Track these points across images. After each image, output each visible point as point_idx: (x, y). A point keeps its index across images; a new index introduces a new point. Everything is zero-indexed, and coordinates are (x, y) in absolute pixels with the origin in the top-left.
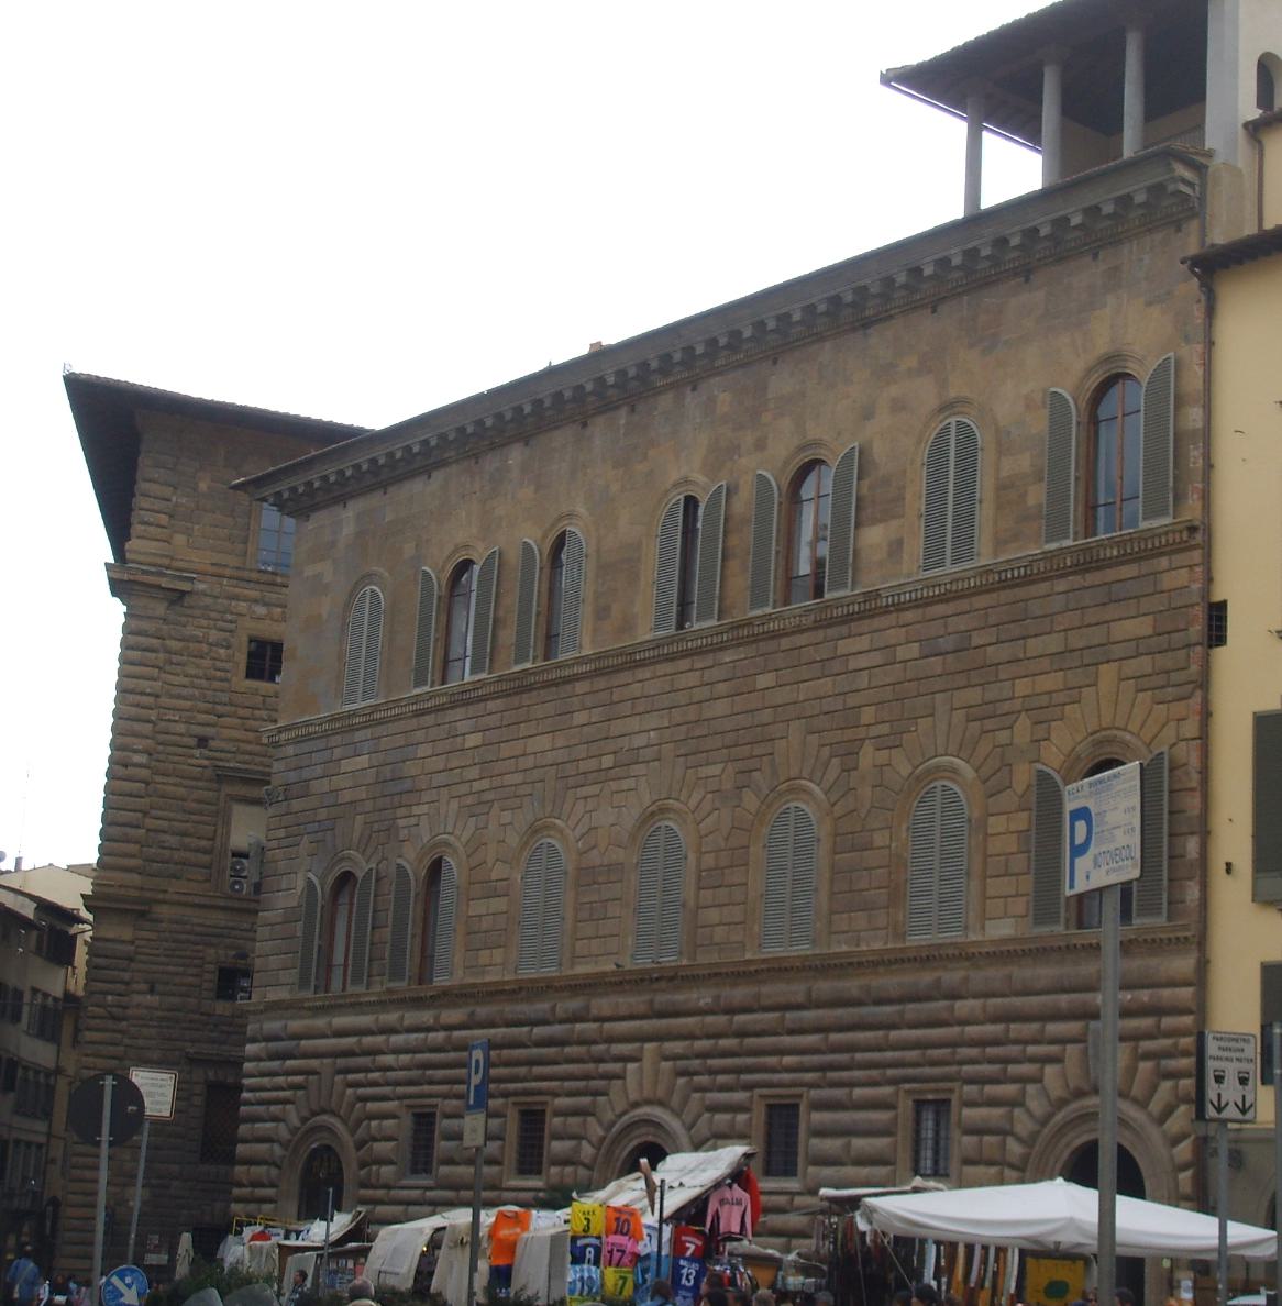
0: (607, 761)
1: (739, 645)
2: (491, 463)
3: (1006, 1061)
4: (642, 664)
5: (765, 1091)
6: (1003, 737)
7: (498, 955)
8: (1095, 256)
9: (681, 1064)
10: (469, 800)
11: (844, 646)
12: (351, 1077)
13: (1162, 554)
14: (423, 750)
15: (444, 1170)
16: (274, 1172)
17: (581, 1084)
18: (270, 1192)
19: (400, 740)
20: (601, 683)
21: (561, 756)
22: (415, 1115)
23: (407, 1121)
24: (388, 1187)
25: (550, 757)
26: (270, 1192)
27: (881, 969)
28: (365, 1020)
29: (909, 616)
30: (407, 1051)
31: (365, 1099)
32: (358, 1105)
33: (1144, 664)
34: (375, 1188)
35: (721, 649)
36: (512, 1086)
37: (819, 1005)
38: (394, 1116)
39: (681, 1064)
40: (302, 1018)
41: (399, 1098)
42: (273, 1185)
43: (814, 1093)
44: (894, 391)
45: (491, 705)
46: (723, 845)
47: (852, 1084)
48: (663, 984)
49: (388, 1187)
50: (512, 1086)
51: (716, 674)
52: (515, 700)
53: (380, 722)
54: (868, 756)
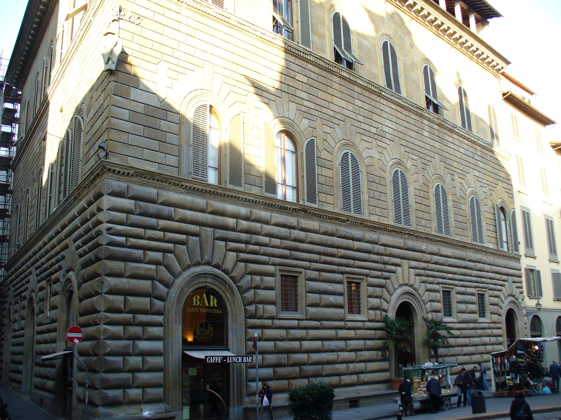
0: (373, 130)
7: (330, 199)
12: (232, 245)
15: (312, 310)
16: (159, 304)
17: (379, 273)
18: (159, 319)
24: (272, 318)
28: (243, 210)
30: (276, 237)
34: (260, 318)
36: (348, 269)
38: (272, 275)
40: (177, 192)
42: (159, 313)
45: (310, 66)
49: (272, 318)
50: (348, 269)
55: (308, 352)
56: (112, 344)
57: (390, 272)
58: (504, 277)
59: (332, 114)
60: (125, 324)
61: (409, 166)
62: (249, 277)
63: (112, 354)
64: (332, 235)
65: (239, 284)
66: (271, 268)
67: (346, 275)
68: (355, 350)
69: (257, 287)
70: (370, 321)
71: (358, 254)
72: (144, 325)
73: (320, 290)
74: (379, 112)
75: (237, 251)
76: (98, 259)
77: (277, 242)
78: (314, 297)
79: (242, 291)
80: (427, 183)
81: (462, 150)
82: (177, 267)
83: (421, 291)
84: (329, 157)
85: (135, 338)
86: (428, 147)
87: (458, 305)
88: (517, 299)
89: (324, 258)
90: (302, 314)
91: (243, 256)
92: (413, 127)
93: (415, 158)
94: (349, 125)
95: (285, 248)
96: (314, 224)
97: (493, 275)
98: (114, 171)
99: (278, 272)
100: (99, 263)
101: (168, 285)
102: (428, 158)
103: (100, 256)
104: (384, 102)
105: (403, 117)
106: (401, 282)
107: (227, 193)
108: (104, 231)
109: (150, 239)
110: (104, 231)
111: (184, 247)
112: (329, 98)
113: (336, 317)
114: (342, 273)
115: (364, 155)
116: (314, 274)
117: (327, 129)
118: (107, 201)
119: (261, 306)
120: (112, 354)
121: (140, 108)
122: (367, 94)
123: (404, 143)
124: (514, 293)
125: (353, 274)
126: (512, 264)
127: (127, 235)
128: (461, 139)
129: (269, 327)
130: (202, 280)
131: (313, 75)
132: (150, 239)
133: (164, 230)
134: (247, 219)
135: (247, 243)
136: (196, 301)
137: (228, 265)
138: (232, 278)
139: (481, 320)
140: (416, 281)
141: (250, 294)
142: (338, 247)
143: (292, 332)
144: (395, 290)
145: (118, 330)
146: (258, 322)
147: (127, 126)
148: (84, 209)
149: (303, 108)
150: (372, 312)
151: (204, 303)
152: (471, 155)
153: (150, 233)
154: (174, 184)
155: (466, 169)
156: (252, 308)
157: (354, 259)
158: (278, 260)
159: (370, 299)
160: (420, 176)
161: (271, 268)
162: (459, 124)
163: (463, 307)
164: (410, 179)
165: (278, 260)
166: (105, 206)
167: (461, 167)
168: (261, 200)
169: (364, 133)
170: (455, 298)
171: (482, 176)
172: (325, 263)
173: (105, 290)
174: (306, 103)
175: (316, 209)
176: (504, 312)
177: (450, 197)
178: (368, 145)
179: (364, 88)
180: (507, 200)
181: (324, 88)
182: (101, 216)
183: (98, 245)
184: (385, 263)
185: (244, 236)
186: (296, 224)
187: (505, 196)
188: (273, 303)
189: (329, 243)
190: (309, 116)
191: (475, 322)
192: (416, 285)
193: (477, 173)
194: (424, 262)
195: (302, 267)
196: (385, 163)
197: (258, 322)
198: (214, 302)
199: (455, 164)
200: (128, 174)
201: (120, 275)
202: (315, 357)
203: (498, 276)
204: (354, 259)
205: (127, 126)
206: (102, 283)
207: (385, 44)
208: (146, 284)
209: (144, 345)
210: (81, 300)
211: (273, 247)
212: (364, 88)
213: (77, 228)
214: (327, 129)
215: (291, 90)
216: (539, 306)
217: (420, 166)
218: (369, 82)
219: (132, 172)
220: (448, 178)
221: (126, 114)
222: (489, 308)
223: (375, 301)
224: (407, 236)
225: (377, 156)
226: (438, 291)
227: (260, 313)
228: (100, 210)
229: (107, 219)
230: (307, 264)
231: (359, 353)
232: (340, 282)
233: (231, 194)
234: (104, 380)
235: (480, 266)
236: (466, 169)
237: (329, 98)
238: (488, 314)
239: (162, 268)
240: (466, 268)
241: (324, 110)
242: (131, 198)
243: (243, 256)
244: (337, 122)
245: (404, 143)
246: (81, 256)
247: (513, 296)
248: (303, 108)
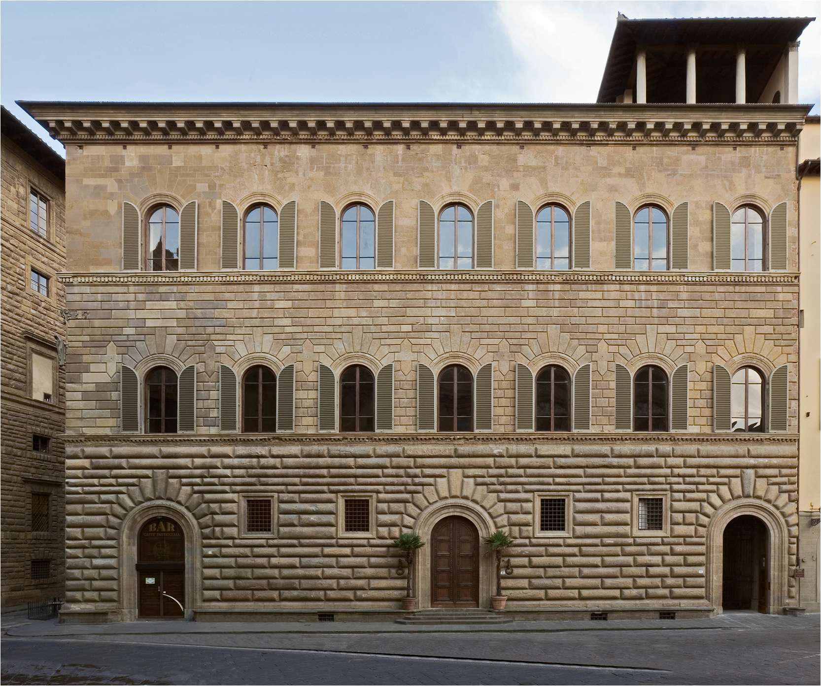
0: (405, 328)
1: (508, 283)
2: (279, 151)
3: (697, 484)
4: (432, 282)
5: (540, 493)
6: (689, 349)
8: (735, 149)
9: (479, 480)
10: (283, 336)
11: (582, 295)
13: (779, 285)
14: (230, 305)
16: (112, 532)
19: (211, 297)
20: (398, 287)
21: (364, 321)
22: (248, 501)
23: (244, 504)
24: (233, 538)
25: (356, 321)
27: (618, 442)
29: (627, 287)
30: (239, 468)
31: (202, 492)
32: (196, 496)
33: (770, 329)
35: (493, 283)
36: (342, 488)
37: (578, 456)
38: (233, 502)
39: (479, 480)
40: (128, 446)
43: (578, 495)
44: (609, 181)
45: (296, 287)
46: (503, 378)
47: (602, 491)
48: (462, 442)
51: (490, 295)
52: (321, 287)
53: (186, 284)
54: (602, 347)
57: (423, 485)
67: (339, 495)
75: (192, 485)
99: (241, 498)
104: (435, 287)
114: (336, 492)
125: (354, 492)
133: (116, 477)
134: (203, 456)
146: (213, 542)
147: (81, 405)
156: (207, 531)
159: (379, 516)
165: (238, 488)
175: (291, 435)
179: (393, 282)
185: (198, 472)
189: (313, 465)
197: (213, 542)
202: (286, 572)
205: (81, 405)
212: (393, 282)
219: (83, 439)
221: (79, 396)
231: (356, 570)
238: (667, 525)
241: (316, 329)
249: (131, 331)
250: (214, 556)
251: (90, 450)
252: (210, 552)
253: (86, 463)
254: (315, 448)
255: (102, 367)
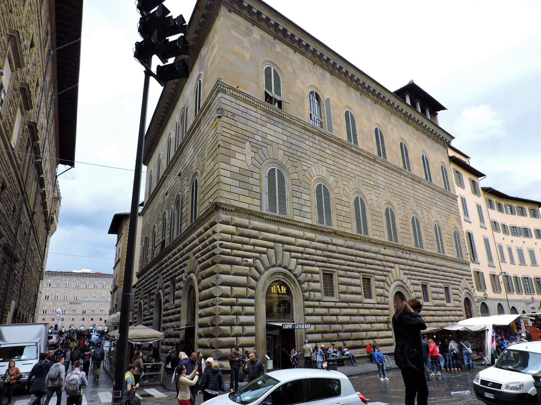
0: (372, 183)
7: (349, 226)
12: (294, 254)
15: (343, 296)
16: (252, 291)
17: (381, 273)
18: (252, 301)
24: (319, 301)
26: (252, 301)
31: (302, 264)
34: (312, 301)
38: (317, 273)
40: (260, 221)
41: (318, 266)
45: (333, 144)
49: (319, 301)
55: (342, 323)
56: (224, 318)
58: (461, 276)
59: (347, 173)
60: (232, 305)
61: (395, 205)
62: (304, 274)
63: (224, 324)
64: (351, 248)
65: (299, 279)
66: (317, 269)
67: (361, 274)
68: (371, 323)
69: (309, 281)
70: (378, 303)
71: (368, 260)
72: (243, 305)
73: (347, 283)
74: (374, 171)
75: (297, 258)
76: (214, 263)
77: (319, 252)
78: (343, 288)
79: (301, 283)
80: (407, 215)
81: (427, 194)
82: (262, 268)
83: (408, 284)
84: (347, 200)
85: (237, 314)
86: (405, 193)
87: (433, 294)
88: (470, 291)
89: (348, 262)
90: (336, 298)
91: (300, 261)
92: (396, 181)
93: (399, 200)
94: (357, 180)
95: (324, 256)
96: (340, 241)
97: (453, 275)
98: (223, 209)
100: (215, 266)
101: (256, 280)
102: (406, 200)
103: (215, 261)
105: (389, 174)
106: (395, 278)
107: (290, 222)
108: (218, 246)
109: (246, 250)
110: (218, 246)
111: (265, 256)
112: (345, 163)
113: (357, 301)
114: (359, 272)
115: (368, 198)
116: (342, 273)
117: (345, 183)
118: (219, 227)
119: (312, 293)
120: (224, 324)
121: (237, 170)
122: (367, 160)
123: (391, 190)
124: (468, 287)
126: (465, 267)
127: (232, 248)
128: (426, 188)
129: (317, 307)
130: (276, 276)
131: (335, 150)
132: (246, 250)
133: (254, 245)
135: (302, 253)
136: (273, 290)
137: (292, 267)
138: (295, 275)
139: (448, 304)
140: (405, 278)
141: (305, 285)
142: (356, 256)
143: (331, 310)
144: (392, 283)
145: (227, 308)
147: (230, 181)
148: (201, 233)
149: (330, 170)
150: (379, 298)
151: (278, 291)
152: (432, 197)
153: (246, 247)
154: (259, 217)
155: (430, 206)
156: (307, 294)
157: (366, 263)
158: (320, 264)
160: (402, 211)
161: (317, 269)
162: (424, 178)
163: (436, 295)
164: (397, 212)
165: (320, 264)
166: (218, 231)
167: (427, 205)
168: (309, 227)
169: (366, 184)
170: (430, 289)
171: (440, 210)
172: (348, 265)
173: (219, 283)
174: (332, 167)
176: (462, 299)
177: (421, 225)
178: (370, 192)
180: (458, 226)
181: (342, 157)
182: (215, 236)
183: (214, 254)
184: (384, 266)
186: (330, 241)
187: (456, 223)
188: (319, 291)
190: (334, 175)
191: (444, 306)
192: (405, 281)
193: (437, 209)
194: (408, 265)
195: (335, 268)
196: (380, 203)
198: (284, 290)
199: (423, 203)
200: (231, 210)
201: (228, 273)
202: (347, 327)
203: (456, 276)
204: (366, 263)
205: (230, 181)
206: (217, 278)
207: (376, 129)
208: (243, 279)
209: (243, 319)
210: (200, 291)
211: (317, 255)
213: (196, 245)
214: (345, 183)
215: (323, 159)
216: (486, 296)
217: (401, 204)
218: (368, 153)
219: (233, 209)
220: (419, 213)
222: (452, 297)
223: (380, 291)
224: (396, 249)
225: (375, 199)
226: (418, 285)
227: (312, 297)
228: (214, 232)
229: (219, 238)
230: (338, 266)
231: (373, 325)
232: (358, 278)
233: (291, 223)
234: (219, 342)
235: (444, 268)
236: (430, 206)
237: (345, 163)
239: (253, 268)
240: (435, 270)
241: (343, 171)
242: (233, 225)
243: (300, 261)
244: (351, 178)
245: (391, 190)
246: (200, 263)
247: (468, 289)
248: (330, 170)
249: (259, 138)
250: (311, 315)
251: (237, 220)
252: (310, 311)
253: (232, 229)
254: (350, 243)
255: (242, 157)
